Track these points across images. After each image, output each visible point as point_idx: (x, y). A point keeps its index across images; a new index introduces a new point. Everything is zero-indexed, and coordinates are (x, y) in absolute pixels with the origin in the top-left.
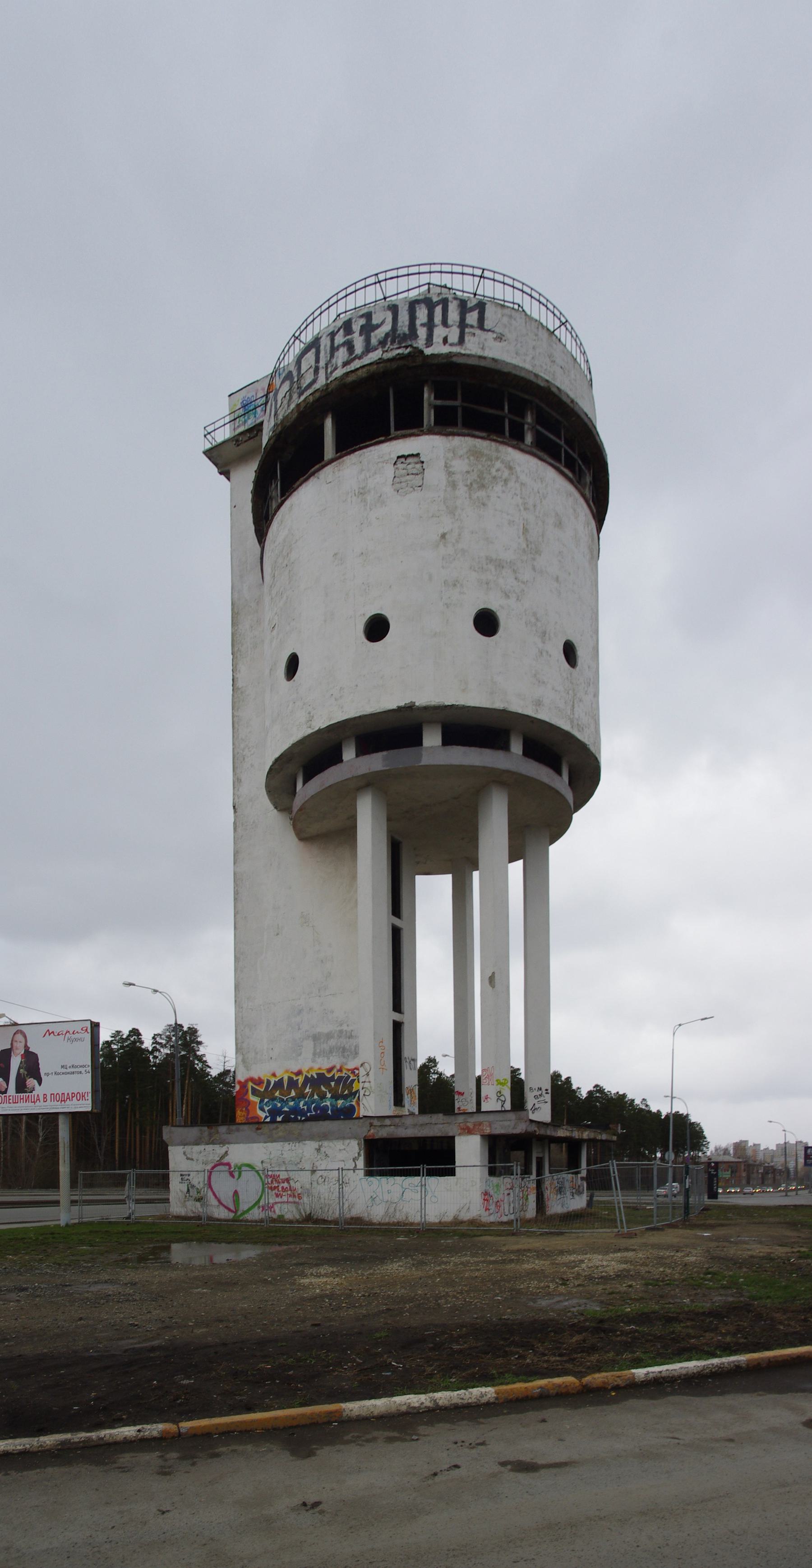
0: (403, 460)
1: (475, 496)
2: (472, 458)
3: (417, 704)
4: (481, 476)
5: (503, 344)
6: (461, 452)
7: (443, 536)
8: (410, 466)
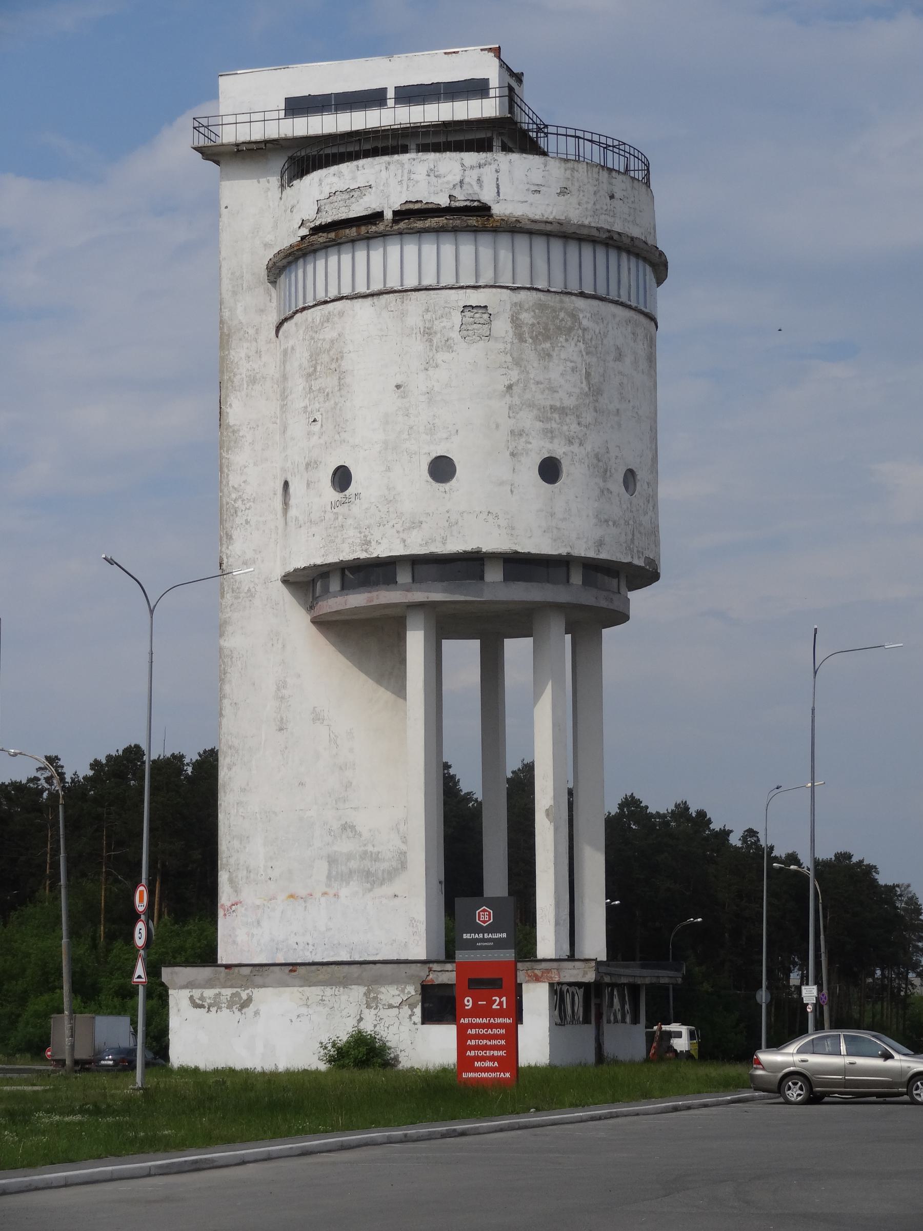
3: (484, 550)
4: (546, 328)
6: (526, 306)
7: (510, 387)
8: (477, 315)
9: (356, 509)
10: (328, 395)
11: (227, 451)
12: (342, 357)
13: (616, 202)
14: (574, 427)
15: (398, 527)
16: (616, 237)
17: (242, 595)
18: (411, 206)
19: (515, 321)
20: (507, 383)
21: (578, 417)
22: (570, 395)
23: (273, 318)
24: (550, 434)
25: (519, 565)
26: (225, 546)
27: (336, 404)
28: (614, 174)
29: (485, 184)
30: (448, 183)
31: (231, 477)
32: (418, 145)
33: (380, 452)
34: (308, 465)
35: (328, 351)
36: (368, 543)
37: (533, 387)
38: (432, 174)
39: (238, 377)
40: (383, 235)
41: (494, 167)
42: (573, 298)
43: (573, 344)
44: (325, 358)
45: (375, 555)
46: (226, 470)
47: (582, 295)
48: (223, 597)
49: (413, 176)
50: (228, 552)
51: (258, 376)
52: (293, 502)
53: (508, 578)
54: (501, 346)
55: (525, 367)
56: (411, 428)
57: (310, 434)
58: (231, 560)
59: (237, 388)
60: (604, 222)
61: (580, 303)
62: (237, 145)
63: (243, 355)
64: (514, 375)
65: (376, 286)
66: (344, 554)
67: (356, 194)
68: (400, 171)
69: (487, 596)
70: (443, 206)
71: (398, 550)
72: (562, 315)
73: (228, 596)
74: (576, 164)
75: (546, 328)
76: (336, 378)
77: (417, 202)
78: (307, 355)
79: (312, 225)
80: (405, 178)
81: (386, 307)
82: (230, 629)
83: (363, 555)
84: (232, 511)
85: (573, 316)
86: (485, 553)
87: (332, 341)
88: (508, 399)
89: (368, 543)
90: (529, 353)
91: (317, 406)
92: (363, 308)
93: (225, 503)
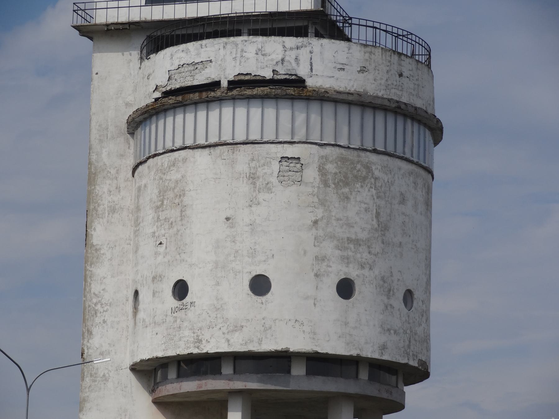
0: (286, 159)
1: (340, 192)
2: (339, 163)
3: (291, 350)
4: (346, 177)
5: (365, 74)
6: (331, 159)
7: (316, 222)
8: (292, 165)
9: (191, 314)
10: (172, 224)
11: (91, 265)
12: (184, 195)
13: (404, 80)
14: (366, 255)
15: (224, 329)
16: (403, 106)
17: (99, 379)
18: (242, 78)
19: (322, 170)
20: (314, 219)
21: (369, 247)
22: (363, 229)
23: (131, 162)
24: (346, 260)
25: (318, 363)
26: (86, 340)
27: (178, 231)
28: (403, 57)
29: (301, 62)
30: (272, 60)
31: (93, 286)
32: (249, 30)
33: (211, 270)
34: (154, 278)
35: (174, 189)
36: (200, 341)
37: (334, 223)
38: (259, 53)
39: (102, 207)
40: (220, 100)
41: (308, 49)
42: (368, 153)
43: (367, 189)
44: (170, 194)
45: (204, 351)
46: (89, 280)
47: (375, 151)
48: (83, 379)
49: (244, 54)
50: (89, 344)
51: (117, 207)
52: (141, 307)
53: (310, 372)
54: (310, 190)
55: (329, 207)
56: (237, 252)
57: (157, 254)
58: (90, 351)
59: (100, 216)
60: (394, 94)
61: (374, 158)
62: (107, 25)
63: (106, 190)
64: (320, 213)
65: (213, 139)
66: (181, 349)
67: (199, 66)
68: (235, 50)
69: (293, 386)
70: (268, 78)
71: (223, 348)
72: (359, 166)
73: (87, 380)
74: (373, 49)
75: (346, 177)
76: (178, 210)
77: (247, 74)
78: (156, 191)
79: (164, 90)
80: (239, 55)
81: (220, 156)
82: (88, 405)
83: (196, 351)
84: (93, 312)
85: (368, 168)
86: (292, 352)
87: (177, 182)
88: (314, 231)
89: (200, 341)
90: (332, 195)
91: (163, 232)
92: (202, 156)
93: (87, 306)
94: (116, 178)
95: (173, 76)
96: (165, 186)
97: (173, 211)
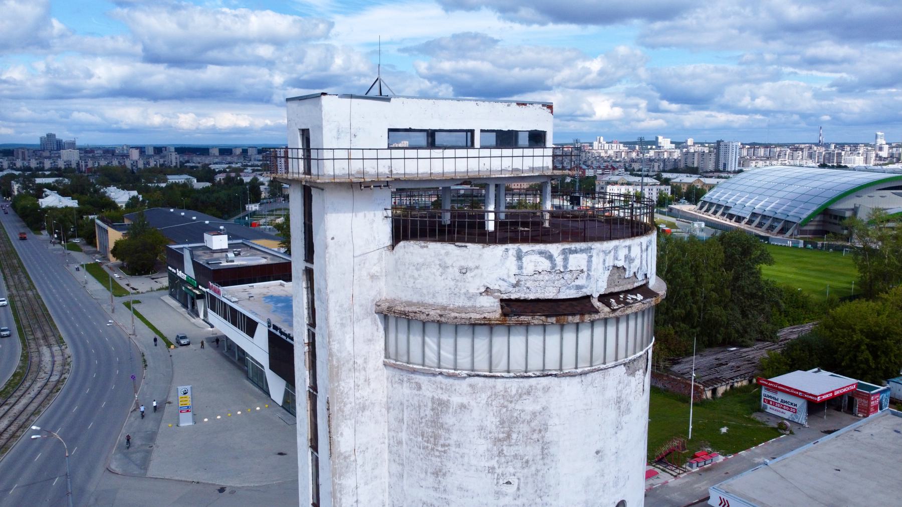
10: (527, 462)
11: (340, 478)
12: (546, 430)
27: (537, 471)
31: (344, 500)
39: (349, 406)
46: (338, 495)
51: (367, 403)
78: (496, 421)
79: (505, 297)
87: (534, 414)
91: (512, 470)
94: (364, 369)
95: (522, 283)
96: (512, 417)
97: (528, 448)
